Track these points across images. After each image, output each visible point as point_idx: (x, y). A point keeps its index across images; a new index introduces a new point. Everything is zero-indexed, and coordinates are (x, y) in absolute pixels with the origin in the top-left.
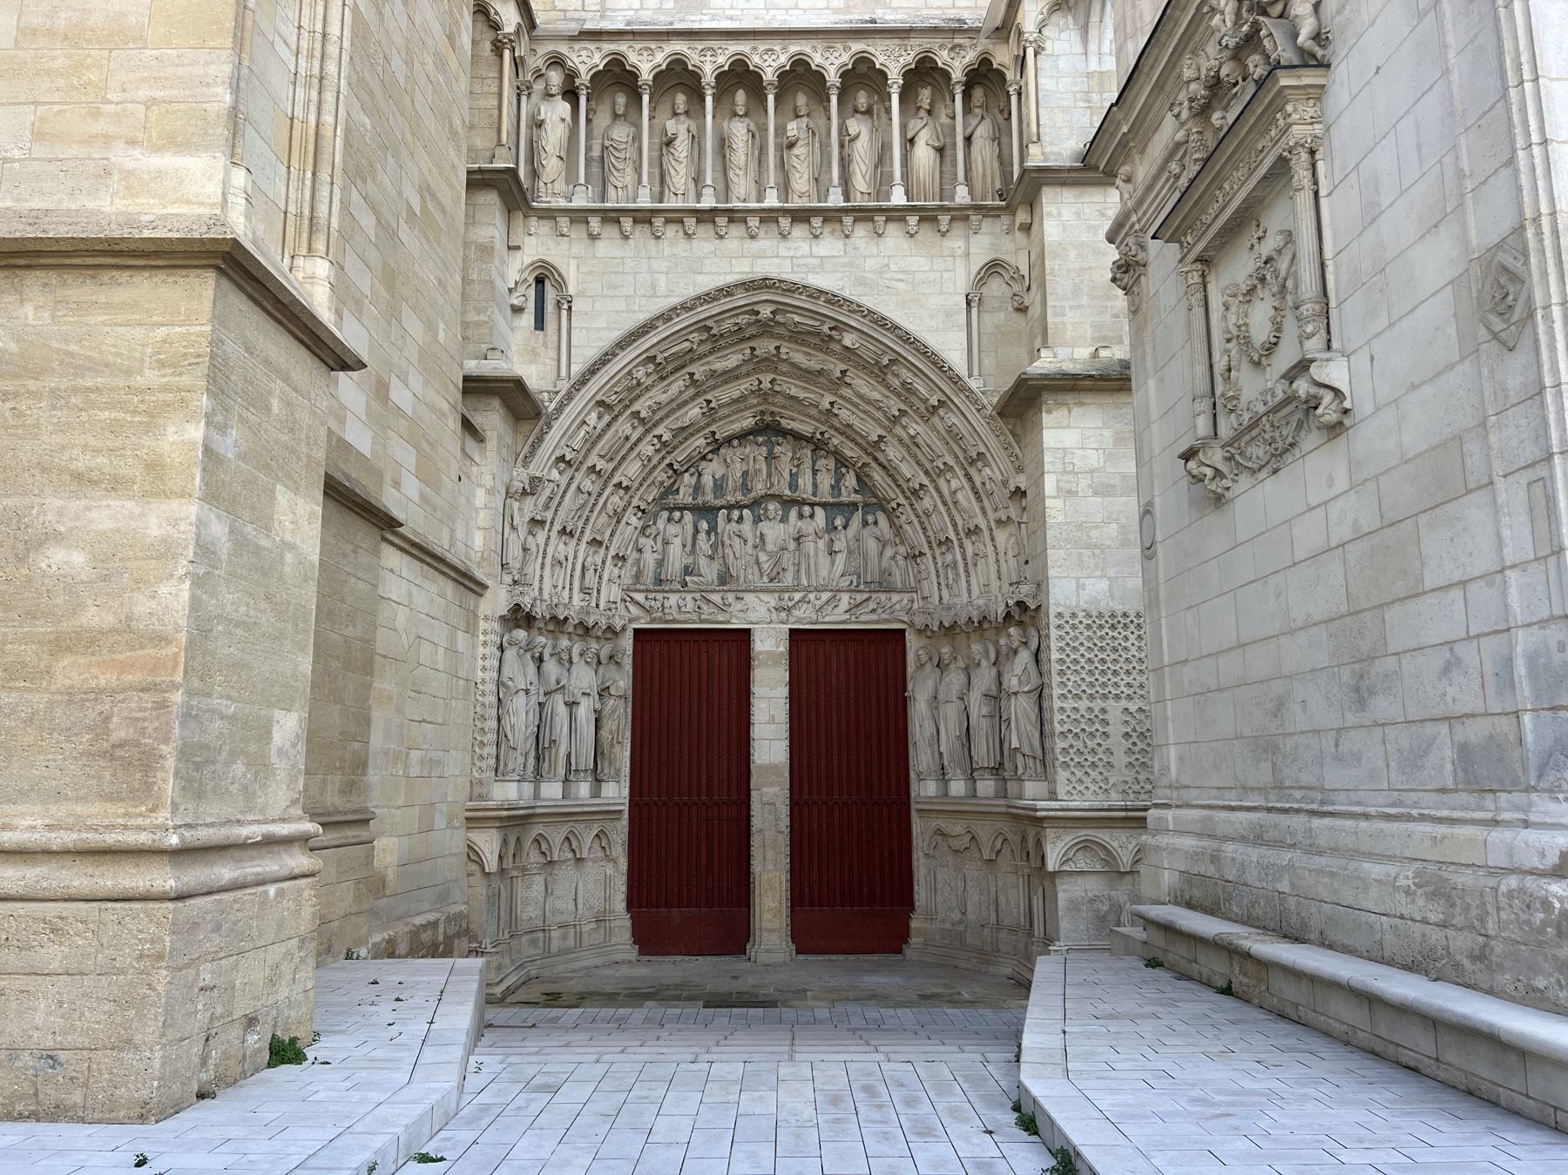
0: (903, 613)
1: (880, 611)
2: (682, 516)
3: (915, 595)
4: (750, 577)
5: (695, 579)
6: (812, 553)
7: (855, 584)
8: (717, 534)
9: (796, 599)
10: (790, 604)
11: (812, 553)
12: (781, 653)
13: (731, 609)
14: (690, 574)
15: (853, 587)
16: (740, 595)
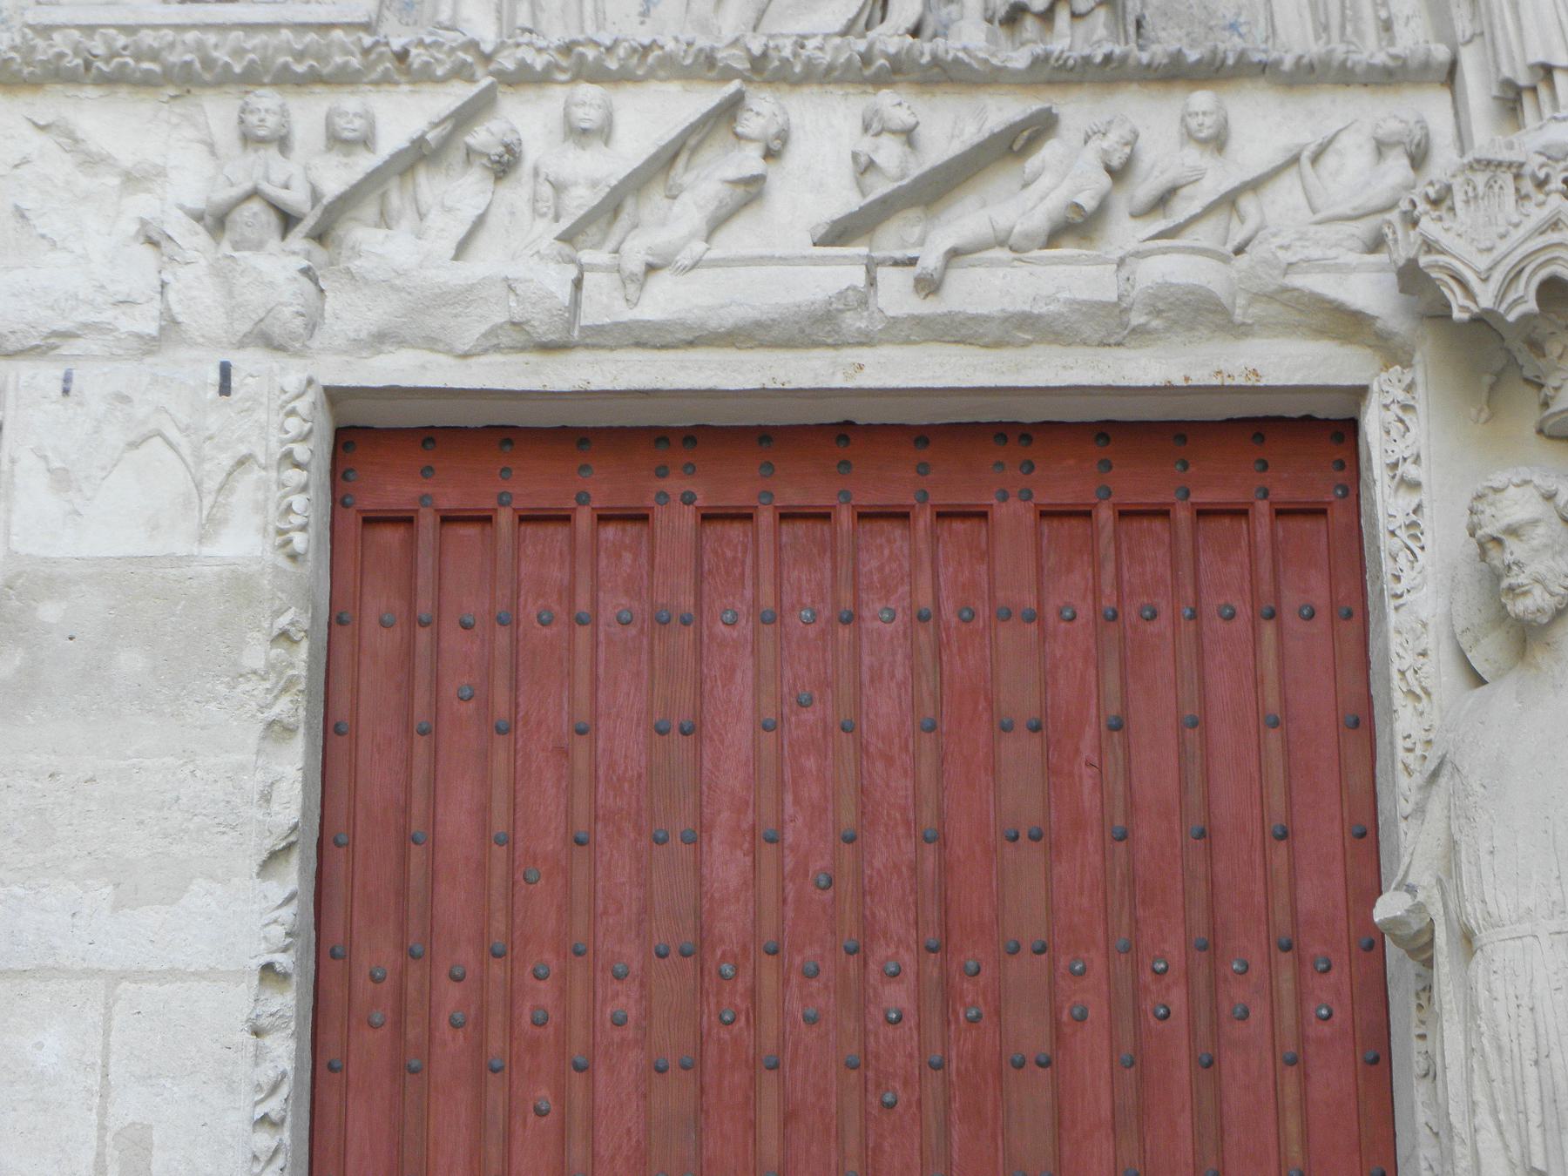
0: (1343, 242)
1: (1125, 233)
3: (1433, 109)
10: (336, 177)
12: (239, 585)
15: (889, 38)
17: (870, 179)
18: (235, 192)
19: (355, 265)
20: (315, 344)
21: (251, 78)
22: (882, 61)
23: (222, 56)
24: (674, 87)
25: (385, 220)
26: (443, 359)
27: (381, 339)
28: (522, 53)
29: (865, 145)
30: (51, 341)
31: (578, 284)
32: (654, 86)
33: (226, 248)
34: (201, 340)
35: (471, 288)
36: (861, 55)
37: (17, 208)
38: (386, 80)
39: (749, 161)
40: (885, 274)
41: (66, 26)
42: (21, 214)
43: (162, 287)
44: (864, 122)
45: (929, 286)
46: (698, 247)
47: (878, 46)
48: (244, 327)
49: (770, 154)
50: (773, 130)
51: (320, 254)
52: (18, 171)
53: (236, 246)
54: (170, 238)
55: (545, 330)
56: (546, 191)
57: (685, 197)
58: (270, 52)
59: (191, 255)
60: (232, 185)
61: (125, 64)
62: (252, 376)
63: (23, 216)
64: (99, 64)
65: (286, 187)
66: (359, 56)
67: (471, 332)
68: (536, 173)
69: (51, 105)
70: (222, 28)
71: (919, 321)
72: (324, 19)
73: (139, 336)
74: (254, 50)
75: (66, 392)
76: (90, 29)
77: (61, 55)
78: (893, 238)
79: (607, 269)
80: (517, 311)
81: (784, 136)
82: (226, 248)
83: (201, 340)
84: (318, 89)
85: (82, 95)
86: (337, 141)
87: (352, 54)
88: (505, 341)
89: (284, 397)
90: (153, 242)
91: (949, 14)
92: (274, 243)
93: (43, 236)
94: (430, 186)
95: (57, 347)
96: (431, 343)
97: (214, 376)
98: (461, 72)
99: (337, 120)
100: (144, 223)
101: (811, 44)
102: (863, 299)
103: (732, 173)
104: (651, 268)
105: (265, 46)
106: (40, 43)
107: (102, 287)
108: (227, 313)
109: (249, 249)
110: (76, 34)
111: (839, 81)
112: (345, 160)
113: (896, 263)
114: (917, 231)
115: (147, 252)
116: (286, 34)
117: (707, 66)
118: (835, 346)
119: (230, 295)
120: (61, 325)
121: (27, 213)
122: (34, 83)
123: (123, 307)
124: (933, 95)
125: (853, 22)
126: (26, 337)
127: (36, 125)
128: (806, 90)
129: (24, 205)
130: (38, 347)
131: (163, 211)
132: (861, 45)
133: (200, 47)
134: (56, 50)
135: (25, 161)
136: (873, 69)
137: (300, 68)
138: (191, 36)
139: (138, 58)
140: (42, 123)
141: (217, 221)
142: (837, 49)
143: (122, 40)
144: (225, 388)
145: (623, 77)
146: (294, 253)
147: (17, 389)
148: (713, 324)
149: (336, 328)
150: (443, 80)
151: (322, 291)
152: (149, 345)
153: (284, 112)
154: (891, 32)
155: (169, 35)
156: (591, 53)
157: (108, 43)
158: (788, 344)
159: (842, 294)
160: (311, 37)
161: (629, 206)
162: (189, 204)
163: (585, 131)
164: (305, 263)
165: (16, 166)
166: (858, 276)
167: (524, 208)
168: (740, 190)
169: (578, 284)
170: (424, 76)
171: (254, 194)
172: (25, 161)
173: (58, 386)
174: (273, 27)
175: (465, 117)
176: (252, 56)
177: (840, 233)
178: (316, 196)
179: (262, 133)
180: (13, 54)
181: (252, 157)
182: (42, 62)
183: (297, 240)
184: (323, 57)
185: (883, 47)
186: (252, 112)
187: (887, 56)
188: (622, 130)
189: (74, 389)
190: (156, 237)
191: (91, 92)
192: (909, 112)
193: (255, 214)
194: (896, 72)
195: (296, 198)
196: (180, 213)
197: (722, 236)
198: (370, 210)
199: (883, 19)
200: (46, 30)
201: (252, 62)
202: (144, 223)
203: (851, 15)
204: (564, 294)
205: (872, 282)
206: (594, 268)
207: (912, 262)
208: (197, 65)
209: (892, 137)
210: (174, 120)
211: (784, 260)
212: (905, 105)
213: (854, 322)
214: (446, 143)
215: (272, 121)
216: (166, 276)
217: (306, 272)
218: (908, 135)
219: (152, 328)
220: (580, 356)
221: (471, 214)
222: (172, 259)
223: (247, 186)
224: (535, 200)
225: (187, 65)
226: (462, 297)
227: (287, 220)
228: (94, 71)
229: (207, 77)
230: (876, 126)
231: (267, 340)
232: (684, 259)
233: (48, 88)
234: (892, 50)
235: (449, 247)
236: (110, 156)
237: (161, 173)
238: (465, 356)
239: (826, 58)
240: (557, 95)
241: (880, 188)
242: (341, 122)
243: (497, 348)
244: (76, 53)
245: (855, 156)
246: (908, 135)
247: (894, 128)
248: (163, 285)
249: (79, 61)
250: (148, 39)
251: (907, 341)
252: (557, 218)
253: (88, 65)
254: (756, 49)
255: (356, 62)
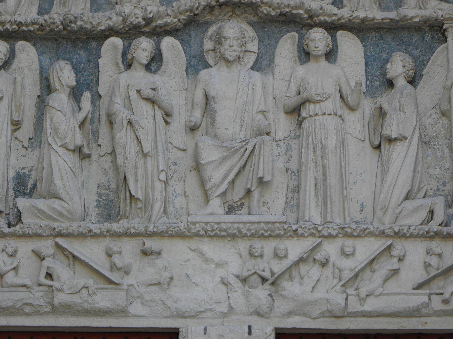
2: (12, 55)
4: (179, 202)
5: (41, 204)
6: (332, 142)
7: (439, 217)
8: (95, 97)
9: (293, 256)
11: (332, 142)
13: (127, 281)
14: (30, 193)
15: (434, 226)
16: (151, 244)
17: (429, 268)
18: (250, 273)
19: (284, 293)
20: (272, 315)
21: (252, 236)
22: (432, 233)
23: (244, 231)
24: (372, 239)
25: (291, 278)
26: (308, 319)
27: (290, 314)
28: (329, 231)
29: (428, 259)
30: (197, 314)
31: (347, 299)
32: (367, 239)
33: (247, 288)
34: (239, 313)
35: (316, 301)
36: (426, 232)
37: (186, 274)
38: (291, 236)
39: (394, 264)
40: (434, 297)
41: (200, 222)
42: (187, 276)
43: (228, 298)
44: (427, 251)
45: (446, 302)
46: (381, 290)
47: (431, 229)
48: (251, 310)
49: (400, 260)
50: (401, 254)
51: (273, 289)
52: (186, 263)
53: (250, 288)
54: (230, 284)
55: (337, 313)
56: (337, 271)
57: (377, 274)
58: (258, 229)
59: (237, 289)
60: (248, 271)
61: (217, 233)
62: (257, 329)
63: (188, 276)
64: (209, 233)
65: (264, 271)
66: (283, 231)
67: (316, 313)
68: (334, 265)
69: (195, 243)
70: (245, 223)
71: (443, 311)
72: (273, 221)
73: (222, 313)
74: (253, 229)
75: (205, 333)
76: (207, 223)
77: (199, 231)
78: (435, 287)
79: (355, 295)
80: (330, 308)
81: (404, 256)
82: (247, 288)
83: (239, 313)
84: (271, 238)
85: (204, 240)
86: (276, 256)
87: (281, 231)
88: (326, 315)
89: (266, 336)
90: (224, 283)
91: (449, 212)
92: (260, 287)
93: (194, 283)
94: (303, 268)
95: (199, 315)
96: (304, 315)
97: (247, 330)
98: (312, 235)
99: (278, 251)
100: (222, 278)
101: (412, 228)
102: (428, 305)
103: (390, 268)
104: (367, 296)
105: (256, 228)
106: (193, 227)
107: (211, 298)
108: (247, 306)
109: (254, 288)
110: (203, 224)
111: (420, 237)
112: (280, 262)
113: (437, 294)
114: (441, 283)
115: (223, 288)
116: (262, 225)
117: (382, 234)
118: (419, 317)
119: (248, 301)
120: (200, 309)
121: (189, 276)
122: (190, 237)
123: (217, 304)
124: (446, 241)
125: (424, 221)
126: (190, 313)
127: (191, 249)
128: (410, 239)
129: (188, 273)
130: (194, 315)
131: (228, 275)
132: (426, 228)
133: (238, 228)
134: (197, 229)
135: (188, 260)
136: (430, 235)
137: (266, 234)
138: (235, 225)
139: (220, 231)
140: (193, 249)
141: (244, 280)
142: (419, 230)
143: (216, 227)
144: (250, 333)
145: (359, 236)
146: (266, 289)
147: (191, 332)
148: (385, 312)
149: (278, 310)
150: (307, 236)
151: (273, 299)
152: (225, 315)
153: (262, 248)
154: (434, 225)
155: (230, 225)
156: (349, 231)
157: (212, 227)
158: (406, 316)
159: (422, 304)
160: (270, 225)
161: (360, 276)
162: (235, 273)
163: (348, 255)
164: (269, 293)
165: (185, 262)
166: (426, 299)
167: (330, 275)
168: (392, 272)
169: (347, 299)
170: (302, 235)
171: (255, 273)
172: (188, 260)
173: (202, 332)
174: (259, 223)
175: (314, 249)
176: (253, 231)
177: (420, 286)
178: (272, 274)
179: (257, 255)
180: (185, 230)
181: (254, 261)
182: (193, 232)
183: (267, 285)
184: (273, 231)
185: (433, 230)
186: (254, 248)
187: (434, 232)
188: (357, 252)
189: (208, 332)
190: (226, 283)
191: (206, 239)
192: (440, 249)
193: (255, 279)
194: (437, 235)
195: (267, 274)
196: (233, 276)
197: (387, 284)
198: (287, 276)
199: (432, 219)
200: (194, 223)
201: (253, 233)
202: (222, 278)
203: (423, 219)
204: (343, 303)
205: (430, 299)
206: (351, 295)
207: (442, 294)
208: (237, 233)
209: (435, 256)
210: (230, 247)
211: (405, 294)
212: (439, 247)
213: (425, 311)
214: (308, 257)
215: (259, 251)
216: (230, 295)
217: (270, 295)
218: (440, 255)
219: (226, 310)
220: (347, 319)
221: (316, 278)
222: (231, 290)
223: (253, 271)
224: (333, 273)
225: (235, 234)
226: (315, 303)
227: (264, 280)
228: (207, 234)
229: (240, 235)
230: (431, 253)
231: (258, 313)
232: (377, 293)
233: (194, 238)
234: (435, 230)
235: (309, 288)
236: (212, 259)
237: (227, 263)
238: (315, 319)
239: (416, 232)
240: (339, 242)
241: (434, 273)
242: (279, 252)
243: (323, 317)
244: (203, 230)
245: (425, 262)
246: (440, 255)
247: (436, 254)
248: (228, 297)
249: (203, 232)
250: (223, 226)
251: (440, 316)
252: (340, 280)
253: (206, 232)
254: (397, 230)
255: (282, 233)
